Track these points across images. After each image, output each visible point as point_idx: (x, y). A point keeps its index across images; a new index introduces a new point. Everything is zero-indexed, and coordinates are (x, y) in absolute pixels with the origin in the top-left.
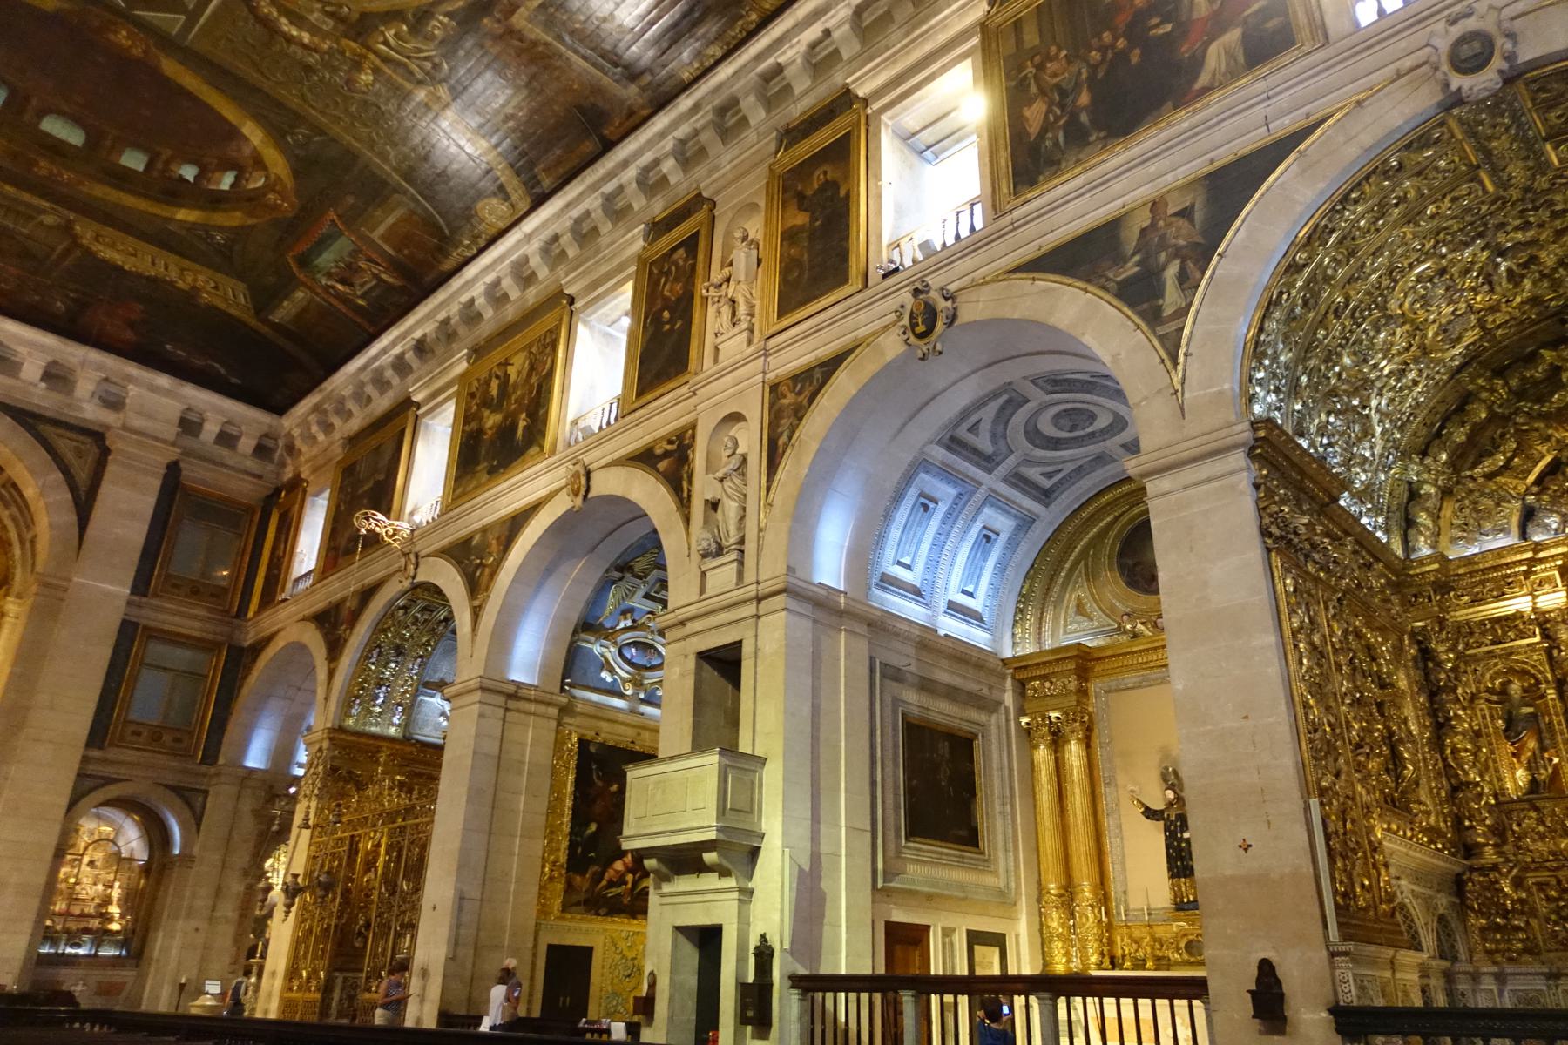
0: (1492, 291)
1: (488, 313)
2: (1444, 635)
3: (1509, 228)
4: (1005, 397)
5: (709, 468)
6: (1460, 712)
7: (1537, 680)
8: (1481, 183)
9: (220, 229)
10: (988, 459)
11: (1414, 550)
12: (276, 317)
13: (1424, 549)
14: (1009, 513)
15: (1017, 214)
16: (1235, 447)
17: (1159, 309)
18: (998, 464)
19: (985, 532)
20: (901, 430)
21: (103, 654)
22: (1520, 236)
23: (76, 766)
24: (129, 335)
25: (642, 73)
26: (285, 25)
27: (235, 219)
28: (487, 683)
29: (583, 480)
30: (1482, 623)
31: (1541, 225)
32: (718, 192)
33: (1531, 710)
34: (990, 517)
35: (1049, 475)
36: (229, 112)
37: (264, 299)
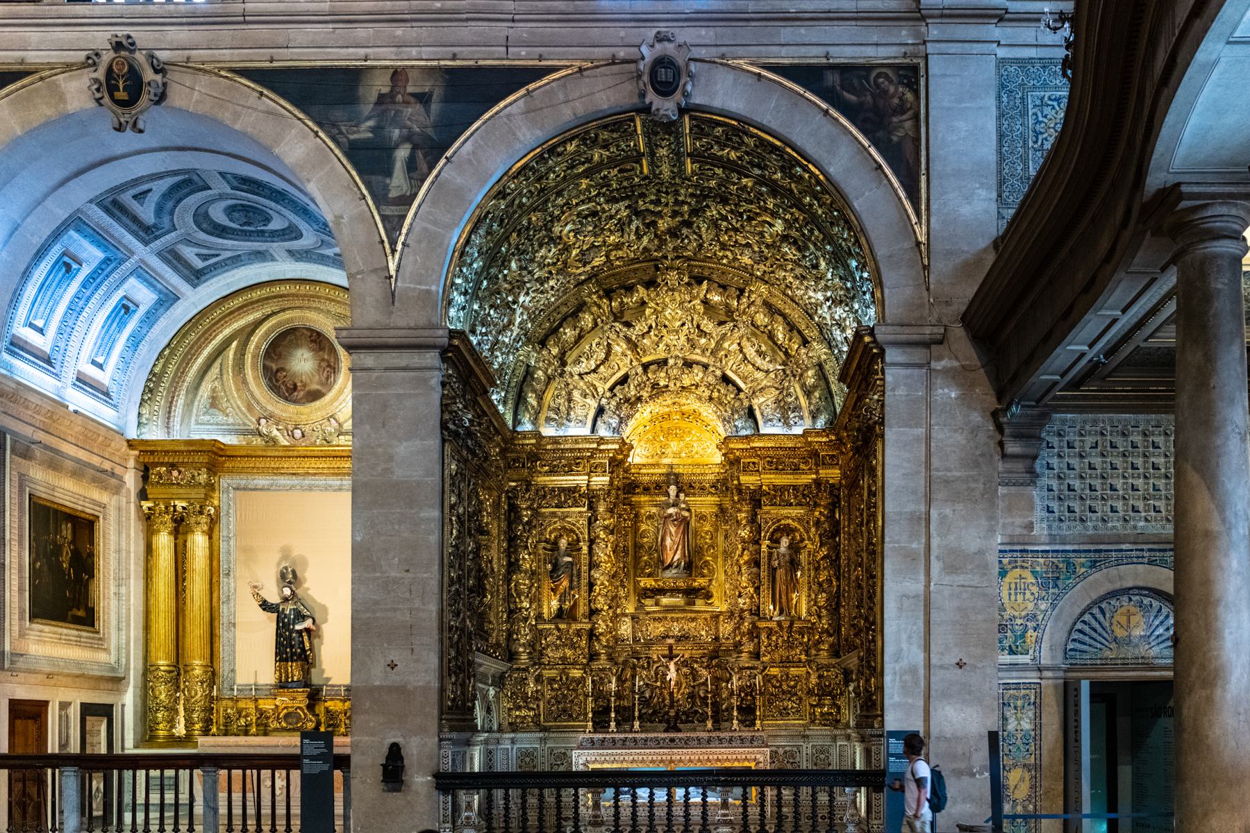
0: (622, 236)
2: (527, 496)
3: (647, 200)
6: (527, 557)
7: (578, 538)
8: (641, 166)
10: (148, 229)
11: (520, 423)
13: (527, 426)
14: (154, 286)
16: (433, 347)
17: (386, 188)
18: (157, 238)
19: (125, 302)
20: (63, 183)
22: (651, 207)
30: (553, 490)
31: (667, 205)
33: (570, 559)
34: (134, 286)
35: (204, 258)
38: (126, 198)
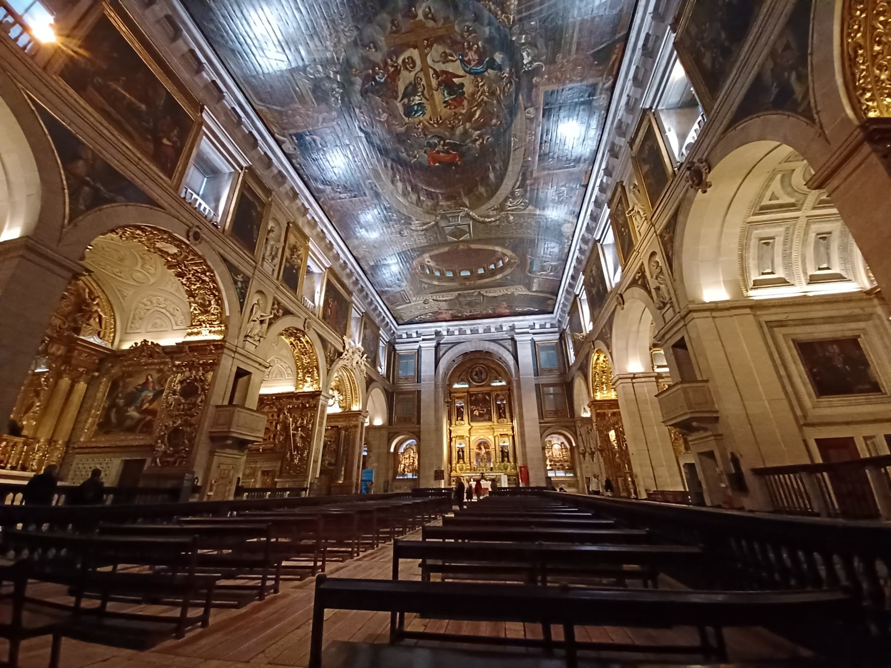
1: (583, 257)
4: (779, 176)
5: (652, 277)
9: (507, 275)
12: (534, 290)
15: (715, 107)
21: (534, 395)
23: (538, 425)
24: (507, 311)
25: (580, 158)
26: (487, 220)
27: (508, 271)
28: (621, 376)
29: (620, 299)
32: (621, 177)
36: (490, 248)
37: (529, 287)
38: (766, 202)
